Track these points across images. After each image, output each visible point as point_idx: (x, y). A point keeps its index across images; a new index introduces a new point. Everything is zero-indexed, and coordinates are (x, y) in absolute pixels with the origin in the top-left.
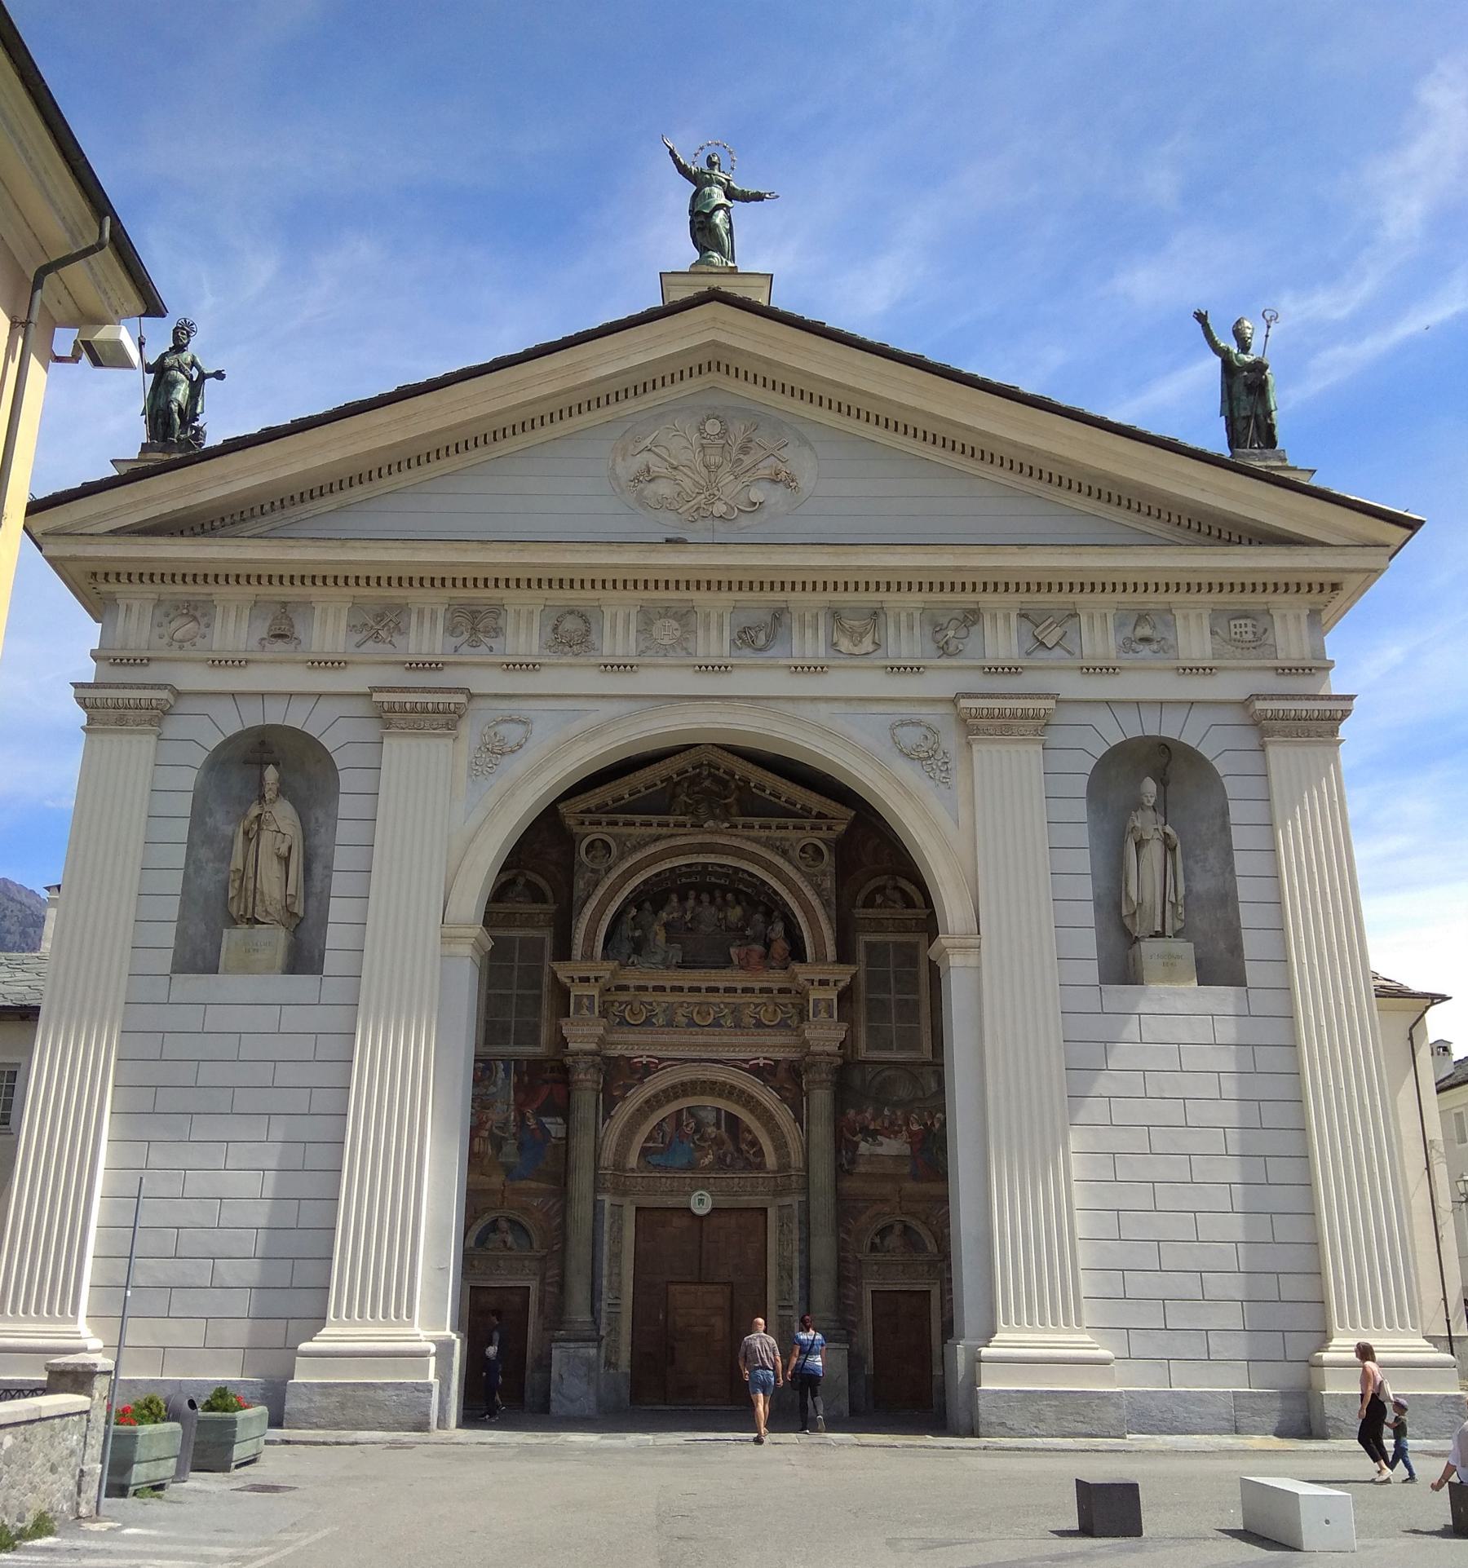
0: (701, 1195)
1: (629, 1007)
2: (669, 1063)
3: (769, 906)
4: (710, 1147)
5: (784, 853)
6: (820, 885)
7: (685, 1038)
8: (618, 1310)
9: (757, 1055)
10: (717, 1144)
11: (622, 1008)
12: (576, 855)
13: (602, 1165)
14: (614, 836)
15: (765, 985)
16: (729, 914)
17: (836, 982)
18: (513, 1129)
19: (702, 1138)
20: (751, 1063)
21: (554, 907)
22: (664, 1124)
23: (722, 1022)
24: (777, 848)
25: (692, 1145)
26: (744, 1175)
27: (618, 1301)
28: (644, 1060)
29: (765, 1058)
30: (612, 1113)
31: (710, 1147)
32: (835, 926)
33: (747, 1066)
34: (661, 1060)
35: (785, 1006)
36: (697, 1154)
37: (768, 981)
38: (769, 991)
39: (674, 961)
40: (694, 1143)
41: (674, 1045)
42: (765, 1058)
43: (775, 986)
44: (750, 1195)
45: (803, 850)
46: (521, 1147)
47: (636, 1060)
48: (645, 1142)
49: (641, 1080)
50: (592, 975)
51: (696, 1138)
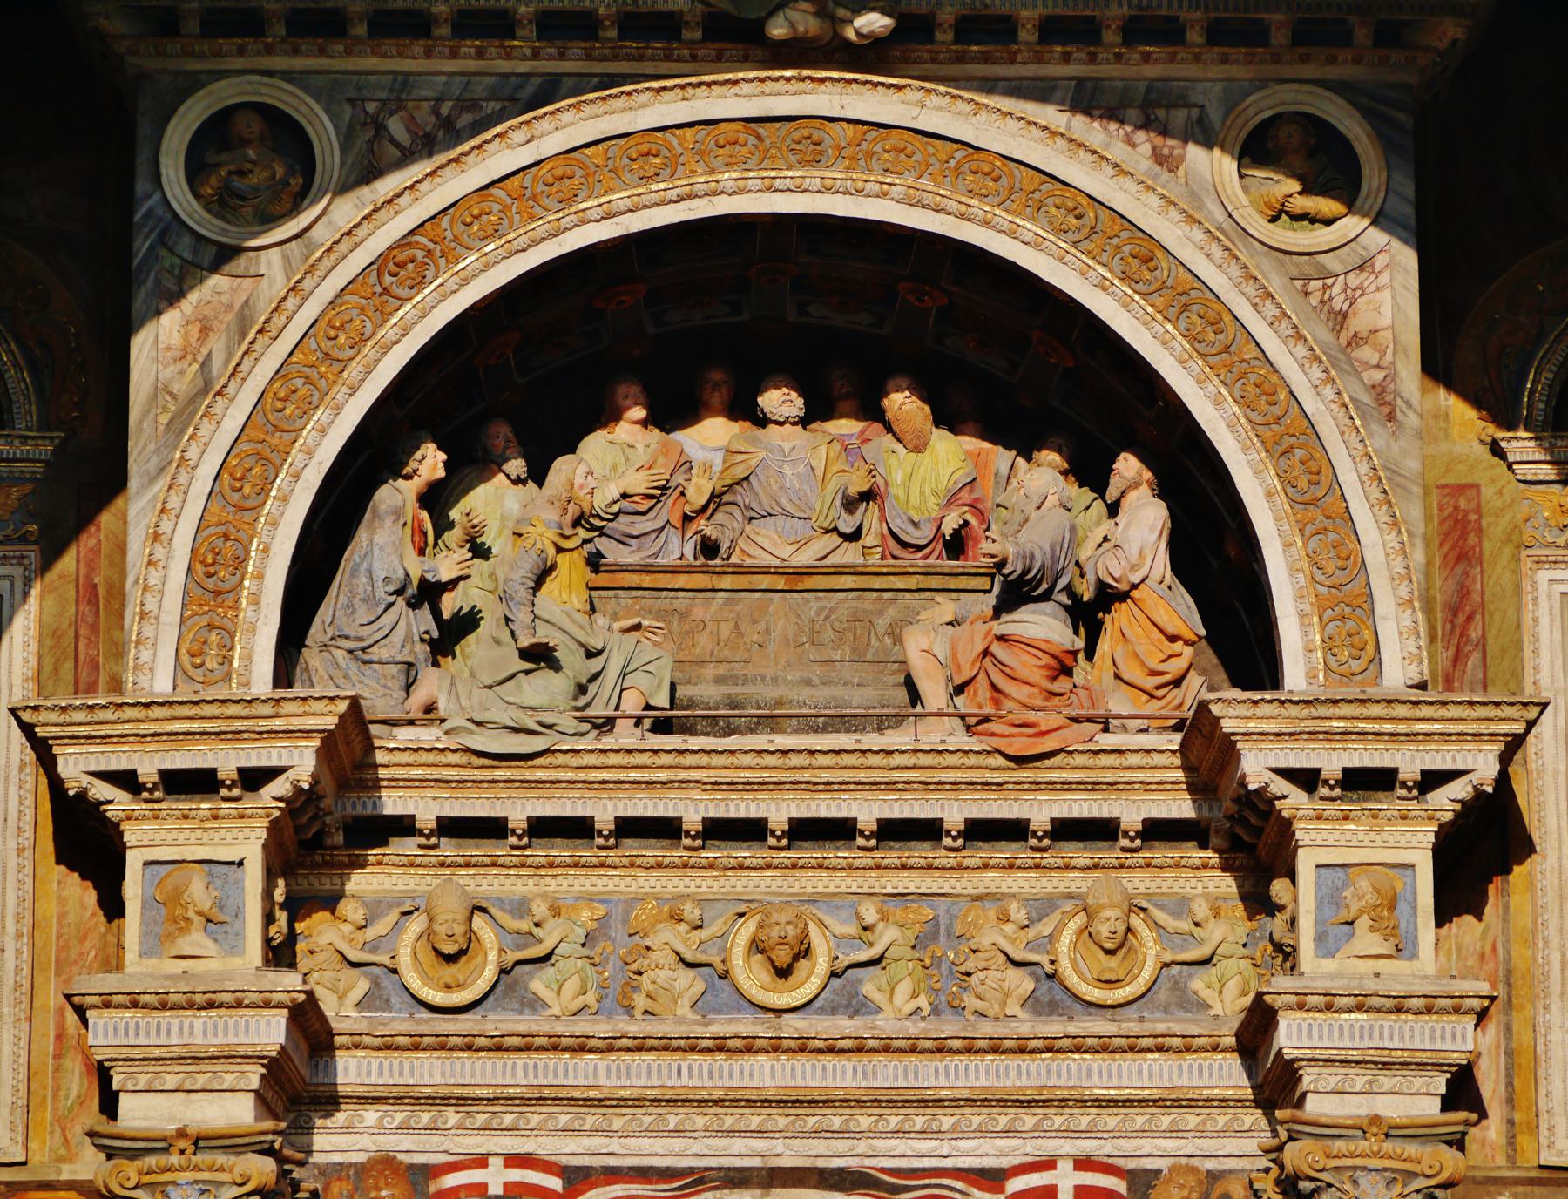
1: (416, 925)
7: (699, 1072)
9: (1049, 1146)
11: (380, 928)
12: (142, 186)
14: (329, 91)
16: (897, 477)
17: (1432, 780)
21: (46, 449)
23: (868, 989)
35: (1181, 906)
37: (1094, 786)
38: (1102, 831)
39: (632, 704)
41: (638, 1102)
47: (451, 1180)
50: (227, 761)
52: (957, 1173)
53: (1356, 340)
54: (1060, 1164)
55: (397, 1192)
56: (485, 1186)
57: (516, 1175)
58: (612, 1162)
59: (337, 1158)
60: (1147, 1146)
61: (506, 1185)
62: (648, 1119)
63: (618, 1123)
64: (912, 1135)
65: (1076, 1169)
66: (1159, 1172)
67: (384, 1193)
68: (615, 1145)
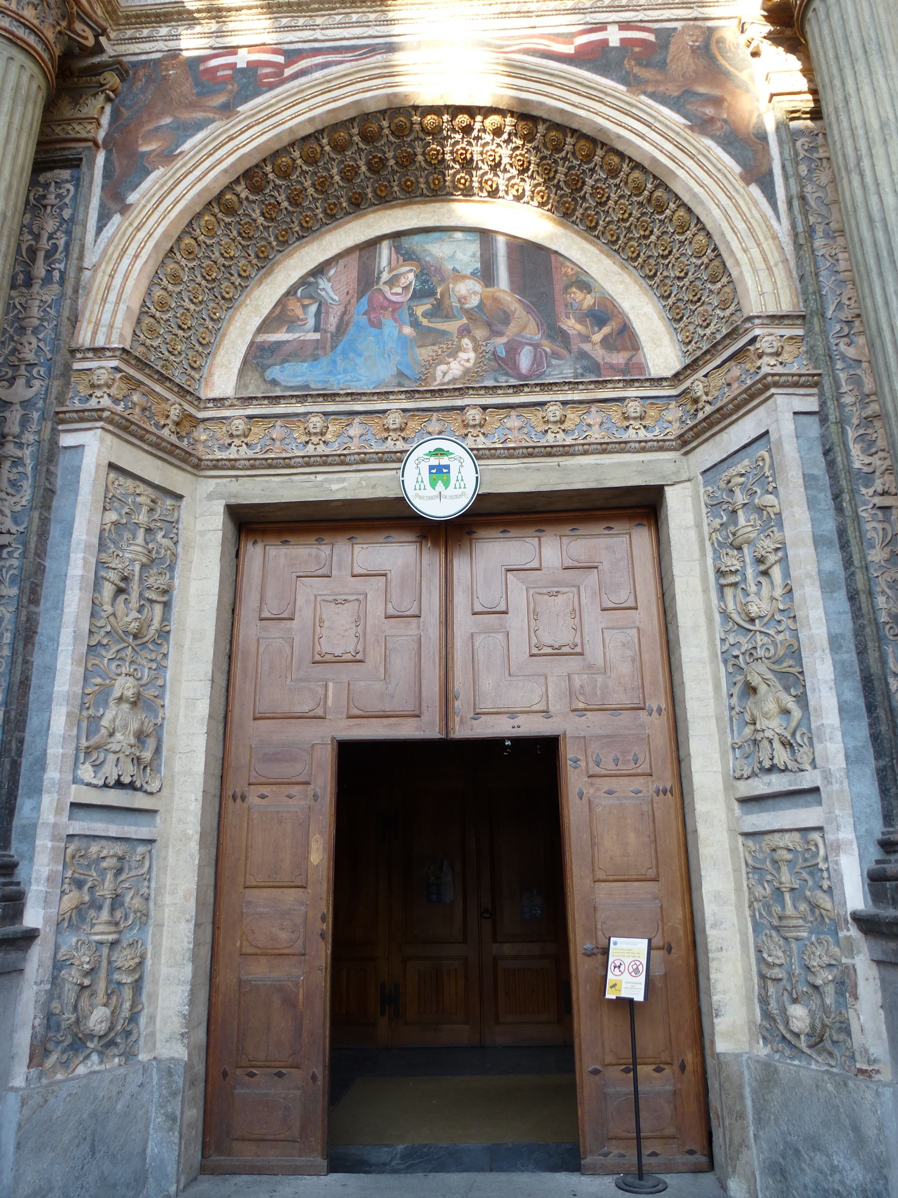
0: (439, 452)
2: (319, 59)
4: (465, 331)
8: (143, 832)
10: (489, 325)
19: (435, 313)
22: (323, 283)
25: (408, 330)
26: (577, 396)
27: (139, 801)
29: (625, 26)
30: (132, 198)
31: (465, 331)
36: (424, 353)
40: (415, 324)
42: (625, 26)
44: (604, 448)
47: (213, 63)
48: (265, 326)
49: (228, 110)
51: (419, 311)
52: (542, 36)
54: (610, 27)
55: (179, 71)
56: (236, 64)
58: (316, 45)
59: (144, 57)
60: (667, 14)
61: (248, 63)
62: (338, 17)
63: (319, 21)
64: (511, 15)
65: (620, 29)
66: (675, 29)
67: (171, 72)
68: (318, 35)
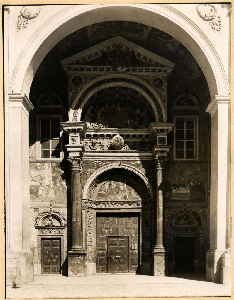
3: (143, 104)
5: (148, 82)
6: (161, 94)
13: (83, 198)
15: (141, 134)
18: (52, 186)
20: (135, 162)
24: (145, 80)
28: (98, 162)
32: (167, 110)
33: (134, 164)
34: (103, 162)
43: (144, 134)
45: (155, 80)
46: (55, 192)
47: (94, 162)
53: (162, 96)
57: (99, 162)
